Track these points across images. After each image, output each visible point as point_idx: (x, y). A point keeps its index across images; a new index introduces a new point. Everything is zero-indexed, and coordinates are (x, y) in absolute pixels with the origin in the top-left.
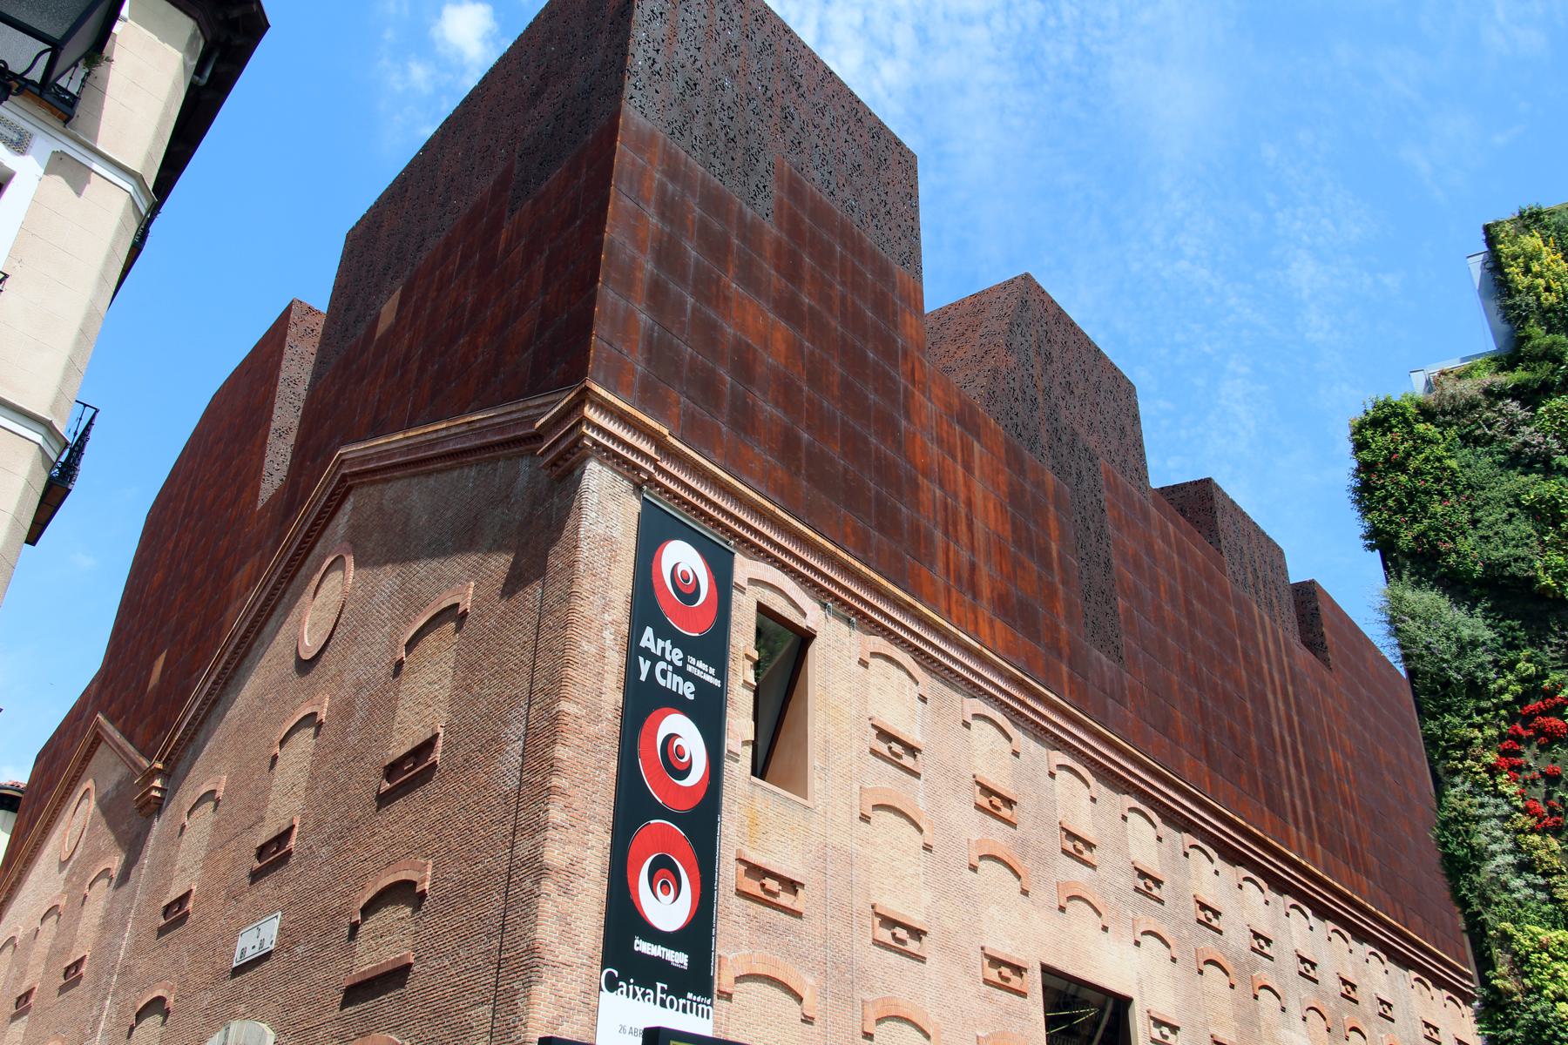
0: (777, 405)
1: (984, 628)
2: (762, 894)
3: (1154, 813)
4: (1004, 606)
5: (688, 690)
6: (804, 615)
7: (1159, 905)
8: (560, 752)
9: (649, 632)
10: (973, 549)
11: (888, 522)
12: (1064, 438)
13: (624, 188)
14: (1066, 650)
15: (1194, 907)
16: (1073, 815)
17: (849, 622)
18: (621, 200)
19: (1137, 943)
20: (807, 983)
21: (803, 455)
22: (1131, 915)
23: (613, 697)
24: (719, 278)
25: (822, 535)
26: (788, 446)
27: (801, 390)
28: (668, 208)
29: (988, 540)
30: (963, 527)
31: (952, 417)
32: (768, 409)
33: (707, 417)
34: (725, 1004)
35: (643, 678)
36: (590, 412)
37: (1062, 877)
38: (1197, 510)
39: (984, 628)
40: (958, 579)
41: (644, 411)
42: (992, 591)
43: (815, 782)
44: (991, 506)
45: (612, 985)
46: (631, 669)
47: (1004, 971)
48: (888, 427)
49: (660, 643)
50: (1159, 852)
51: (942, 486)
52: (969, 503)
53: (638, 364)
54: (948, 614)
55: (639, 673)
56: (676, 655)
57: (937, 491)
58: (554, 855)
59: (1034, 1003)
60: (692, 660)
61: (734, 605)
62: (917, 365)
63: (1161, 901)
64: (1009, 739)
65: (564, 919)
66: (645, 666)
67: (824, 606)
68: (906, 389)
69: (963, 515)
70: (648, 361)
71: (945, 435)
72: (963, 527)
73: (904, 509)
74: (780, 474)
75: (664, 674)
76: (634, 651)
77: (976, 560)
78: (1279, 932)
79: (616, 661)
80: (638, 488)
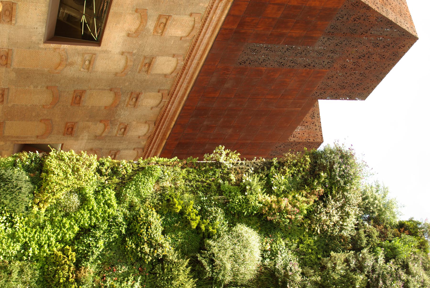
3: (176, 74)
7: (138, 70)
15: (138, 91)
16: (175, 25)
19: (123, 53)
38: (309, 134)
50: (159, 74)
63: (139, 72)
78: (126, 142)
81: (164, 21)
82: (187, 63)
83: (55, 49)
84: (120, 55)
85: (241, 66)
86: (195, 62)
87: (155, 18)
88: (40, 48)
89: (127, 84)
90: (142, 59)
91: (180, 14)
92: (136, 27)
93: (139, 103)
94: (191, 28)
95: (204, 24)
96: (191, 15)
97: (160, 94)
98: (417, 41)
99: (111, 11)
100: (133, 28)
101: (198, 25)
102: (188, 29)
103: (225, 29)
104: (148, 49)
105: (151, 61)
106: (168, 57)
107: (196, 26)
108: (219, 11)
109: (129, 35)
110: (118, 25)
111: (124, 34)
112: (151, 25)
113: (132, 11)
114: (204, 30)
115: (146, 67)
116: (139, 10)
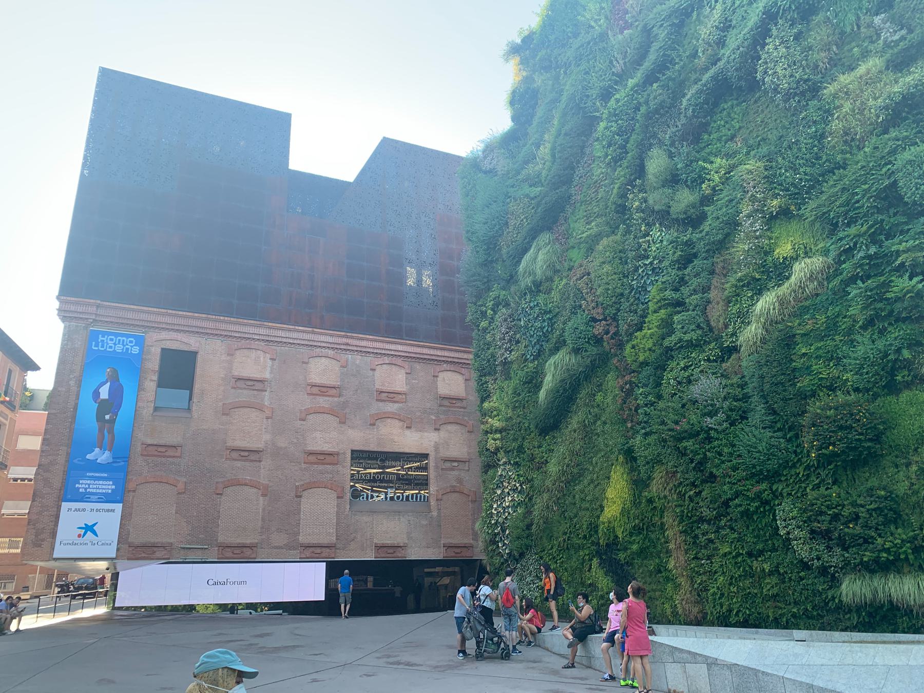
2: (156, 453)
3: (463, 369)
7: (462, 410)
22: (434, 418)
37: (373, 412)
59: (343, 467)
82: (443, 361)
83: (437, 500)
84: (440, 431)
86: (439, 353)
87: (381, 404)
88: (439, 515)
90: (444, 408)
91: (374, 381)
92: (397, 421)
94: (393, 366)
95: (384, 354)
96: (373, 370)
98: (386, 137)
99: (376, 449)
100: (397, 423)
101: (387, 359)
102: (394, 368)
104: (428, 405)
105: (445, 398)
106: (438, 382)
107: (388, 362)
108: (364, 343)
110: (396, 440)
111: (408, 432)
112: (391, 407)
113: (374, 429)
114: (392, 353)
115: (454, 402)
116: (372, 422)
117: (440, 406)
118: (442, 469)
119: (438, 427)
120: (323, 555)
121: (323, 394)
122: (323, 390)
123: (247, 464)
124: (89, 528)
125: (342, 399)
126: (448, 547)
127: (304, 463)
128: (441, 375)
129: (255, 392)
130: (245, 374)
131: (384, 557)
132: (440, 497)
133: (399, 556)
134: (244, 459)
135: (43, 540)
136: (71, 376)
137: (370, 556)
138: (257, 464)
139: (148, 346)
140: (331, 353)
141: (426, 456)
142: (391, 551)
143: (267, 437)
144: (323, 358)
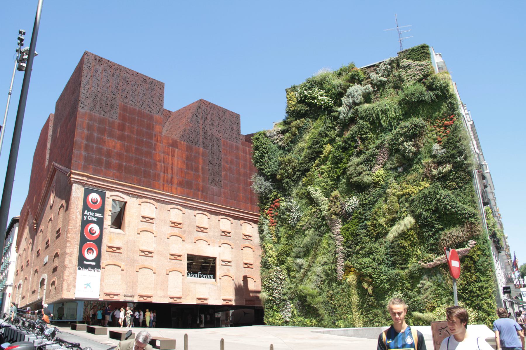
0: (117, 159)
1: (174, 190)
4: (181, 184)
5: (95, 219)
6: (124, 199)
8: (69, 235)
9: (86, 211)
10: (172, 174)
11: (147, 175)
12: (208, 138)
13: (79, 128)
14: (201, 189)
17: (136, 198)
18: (78, 131)
19: (220, 246)
20: (123, 265)
21: (123, 168)
22: (218, 240)
23: (79, 223)
24: (103, 138)
25: (128, 183)
26: (119, 167)
27: (124, 154)
28: (89, 127)
29: (178, 171)
30: (170, 170)
31: (169, 145)
32: (114, 161)
33: (99, 168)
34: (104, 269)
35: (85, 219)
36: (72, 176)
39: (174, 190)
40: (167, 181)
41: (84, 172)
42: (178, 181)
43: (126, 229)
44: (180, 163)
45: (79, 269)
46: (83, 218)
47: (176, 257)
48: (149, 154)
49: (89, 213)
51: (164, 162)
52: (172, 164)
53: (82, 163)
54: (163, 190)
55: (84, 218)
56: (92, 214)
57: (163, 164)
58: (68, 251)
60: (96, 214)
61: (106, 201)
62: (159, 137)
64: (182, 211)
65: (70, 260)
66: (85, 217)
67: (129, 196)
68: (155, 143)
69: (170, 167)
70: (85, 162)
71: (166, 151)
72: (170, 170)
73: (152, 171)
74: (117, 174)
75: (90, 218)
76: (83, 215)
77: (173, 176)
79: (79, 218)
80: (84, 186)
81: (199, 230)
85: (222, 186)
88: (220, 286)
89: (238, 242)
93: (250, 234)
96: (195, 216)
97: (243, 224)
101: (201, 212)
103: (201, 198)
109: (209, 245)
112: (202, 235)
117: (221, 235)
118: (222, 265)
119: (220, 245)
120: (177, 301)
121: (176, 227)
122: (175, 225)
123: (147, 257)
124: (88, 285)
125: (183, 229)
126: (224, 300)
127: (170, 259)
128: (221, 220)
129: (150, 224)
130: (146, 215)
131: (199, 302)
132: (221, 277)
133: (205, 302)
134: (146, 256)
135: (70, 289)
136: (77, 211)
137: (195, 302)
138: (152, 258)
139: (107, 198)
140: (179, 207)
141: (215, 258)
142: (202, 300)
143: (154, 245)
144: (176, 209)
